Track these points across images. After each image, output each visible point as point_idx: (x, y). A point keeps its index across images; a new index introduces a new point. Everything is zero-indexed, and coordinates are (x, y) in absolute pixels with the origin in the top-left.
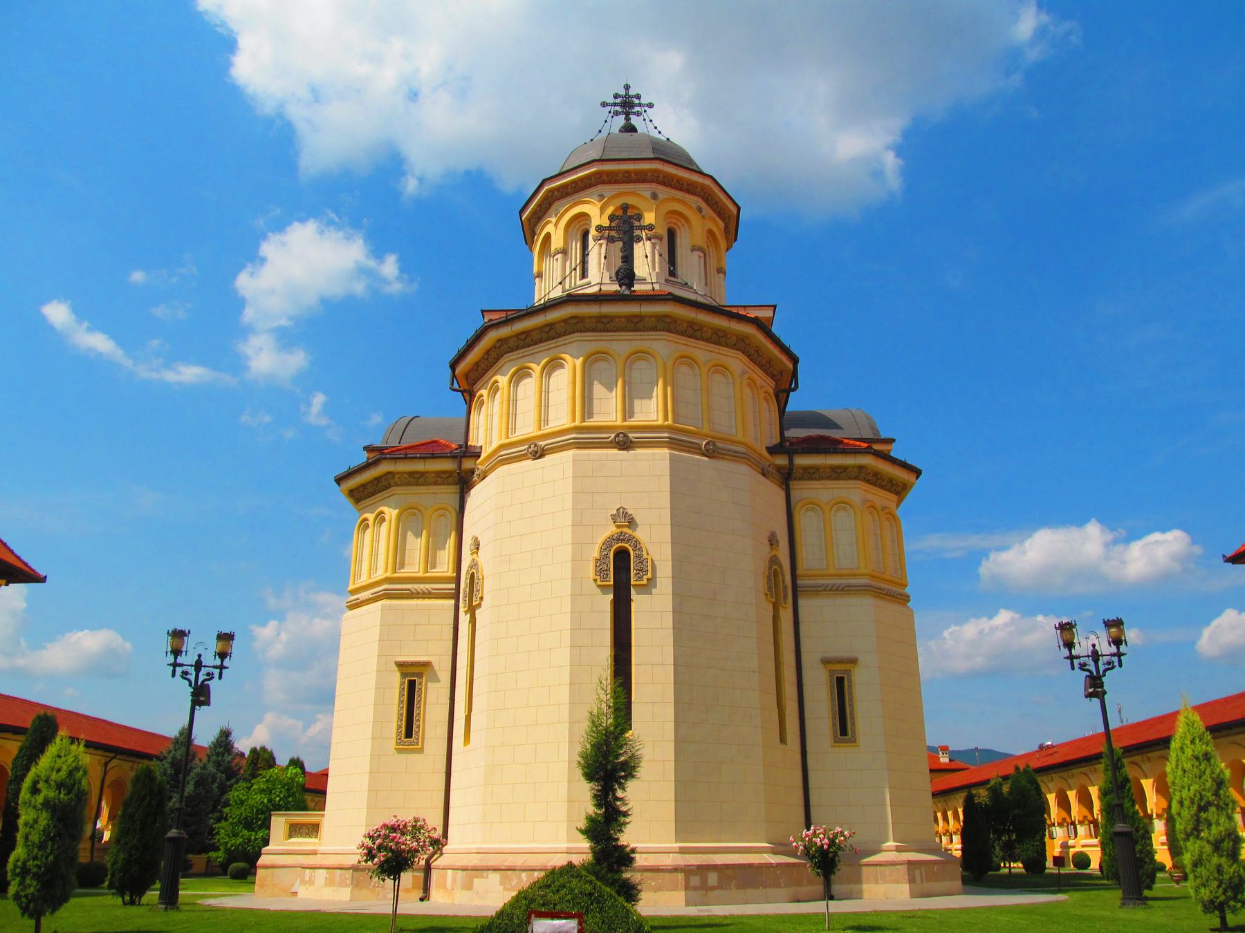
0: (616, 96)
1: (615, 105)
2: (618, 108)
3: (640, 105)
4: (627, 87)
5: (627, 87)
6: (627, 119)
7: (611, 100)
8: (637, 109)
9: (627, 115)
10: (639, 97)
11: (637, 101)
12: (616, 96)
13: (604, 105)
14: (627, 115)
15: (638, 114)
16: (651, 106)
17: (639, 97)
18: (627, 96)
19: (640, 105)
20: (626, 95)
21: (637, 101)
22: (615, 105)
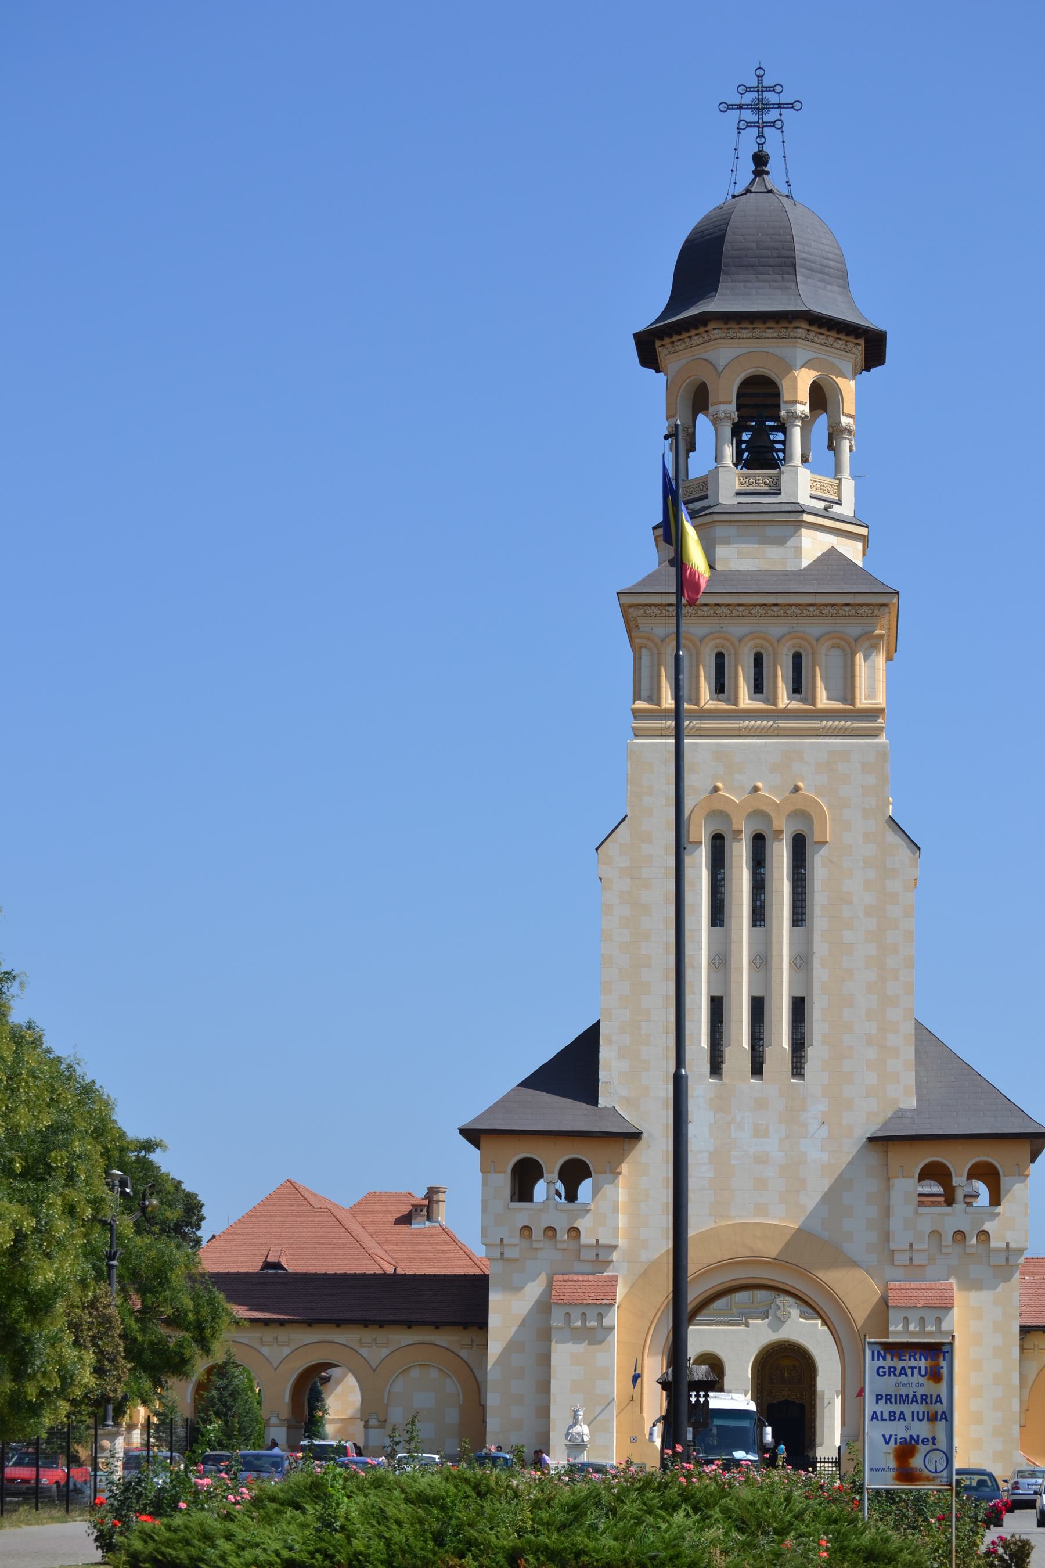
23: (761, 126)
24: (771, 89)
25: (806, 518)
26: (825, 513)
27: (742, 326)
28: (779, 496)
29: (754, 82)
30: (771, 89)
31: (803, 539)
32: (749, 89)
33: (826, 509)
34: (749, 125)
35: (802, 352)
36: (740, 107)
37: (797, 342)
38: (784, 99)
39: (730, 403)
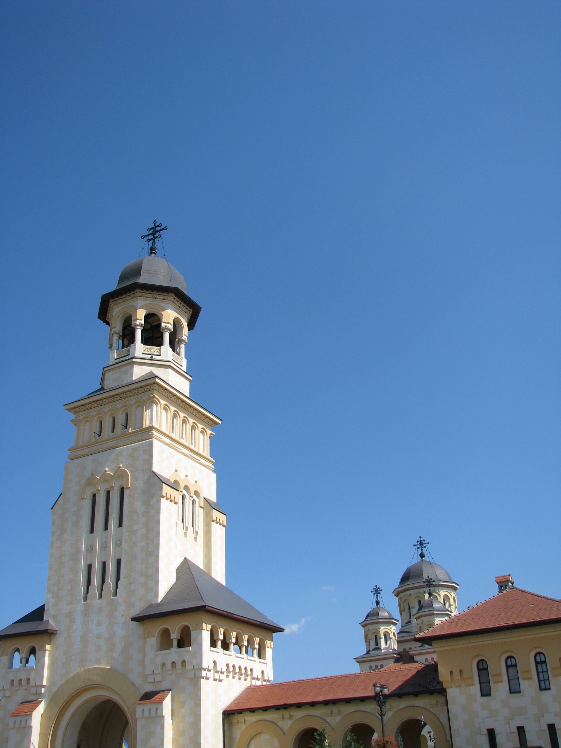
0: (418, 542)
1: (417, 545)
2: (418, 546)
3: (426, 544)
4: (420, 537)
5: (420, 537)
6: (422, 550)
7: (416, 543)
8: (424, 545)
9: (422, 548)
10: (424, 540)
11: (424, 542)
12: (418, 542)
13: (414, 545)
14: (422, 548)
15: (425, 547)
16: (428, 543)
17: (424, 540)
18: (421, 541)
19: (426, 544)
20: (421, 540)
21: (424, 542)
22: (417, 545)
23: (153, 240)
24: (158, 226)
25: (135, 360)
26: (151, 359)
27: (119, 298)
28: (129, 356)
29: (153, 226)
30: (158, 226)
31: (134, 369)
32: (151, 229)
33: (152, 357)
34: (151, 240)
35: (140, 302)
36: (148, 235)
37: (138, 298)
38: (162, 228)
39: (116, 327)
